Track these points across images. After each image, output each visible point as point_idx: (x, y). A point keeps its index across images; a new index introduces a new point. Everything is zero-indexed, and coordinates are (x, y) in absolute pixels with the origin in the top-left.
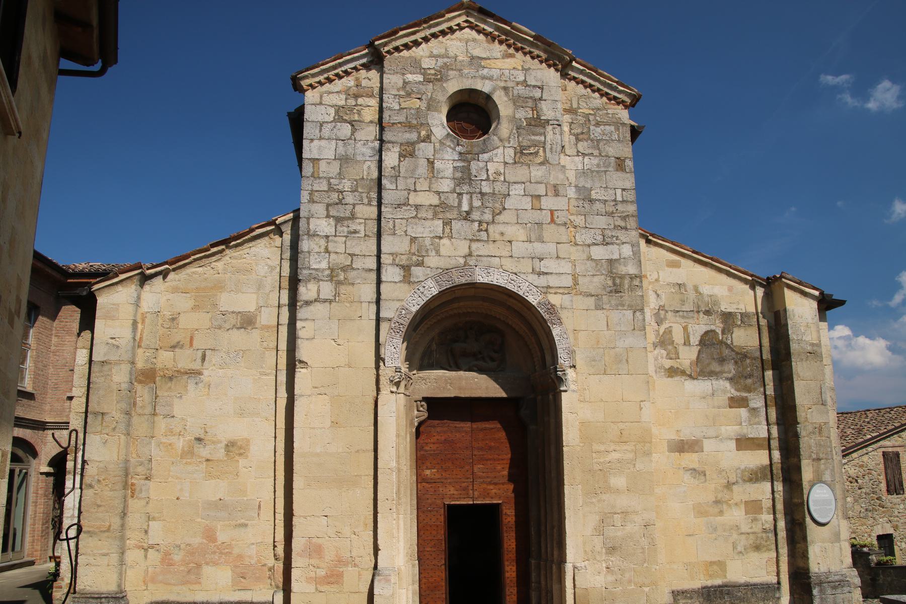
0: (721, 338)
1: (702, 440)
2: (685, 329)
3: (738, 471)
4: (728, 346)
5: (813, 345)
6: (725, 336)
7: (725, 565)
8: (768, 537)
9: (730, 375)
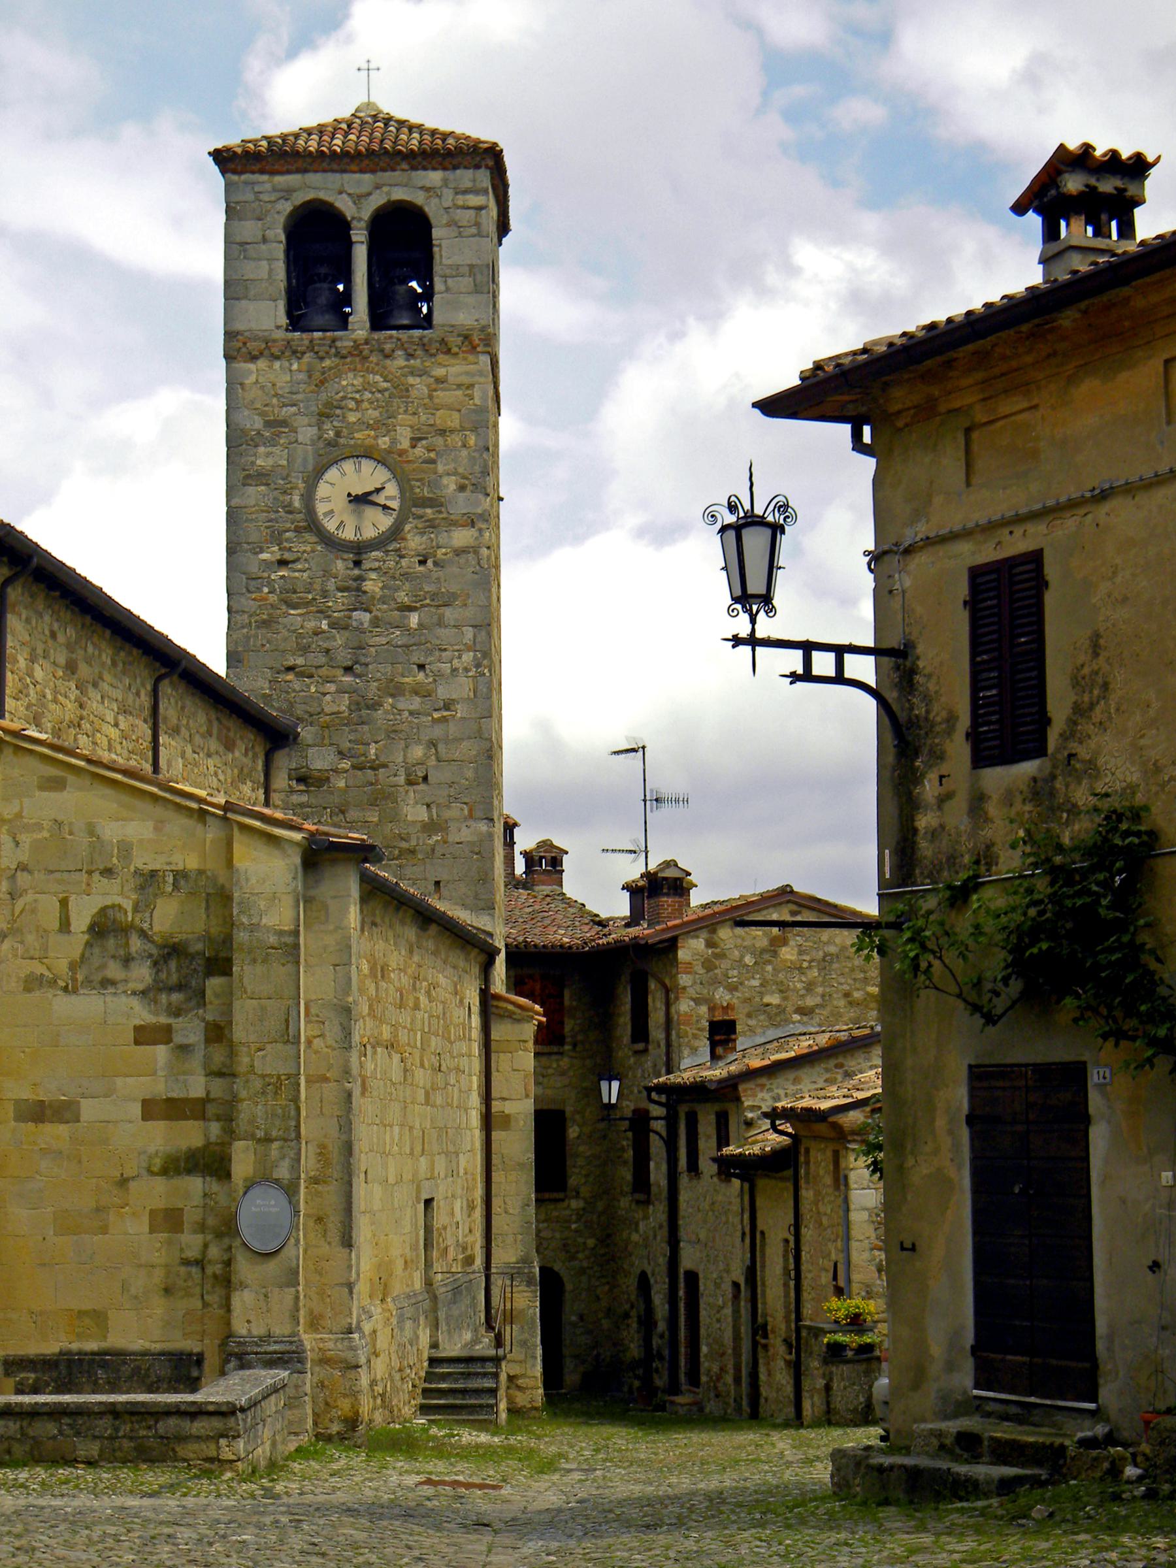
0: (130, 919)
1: (79, 1102)
2: (64, 903)
3: (143, 1157)
4: (143, 934)
5: (281, 933)
6: (139, 915)
7: (106, 1318)
8: (189, 1273)
9: (141, 987)
